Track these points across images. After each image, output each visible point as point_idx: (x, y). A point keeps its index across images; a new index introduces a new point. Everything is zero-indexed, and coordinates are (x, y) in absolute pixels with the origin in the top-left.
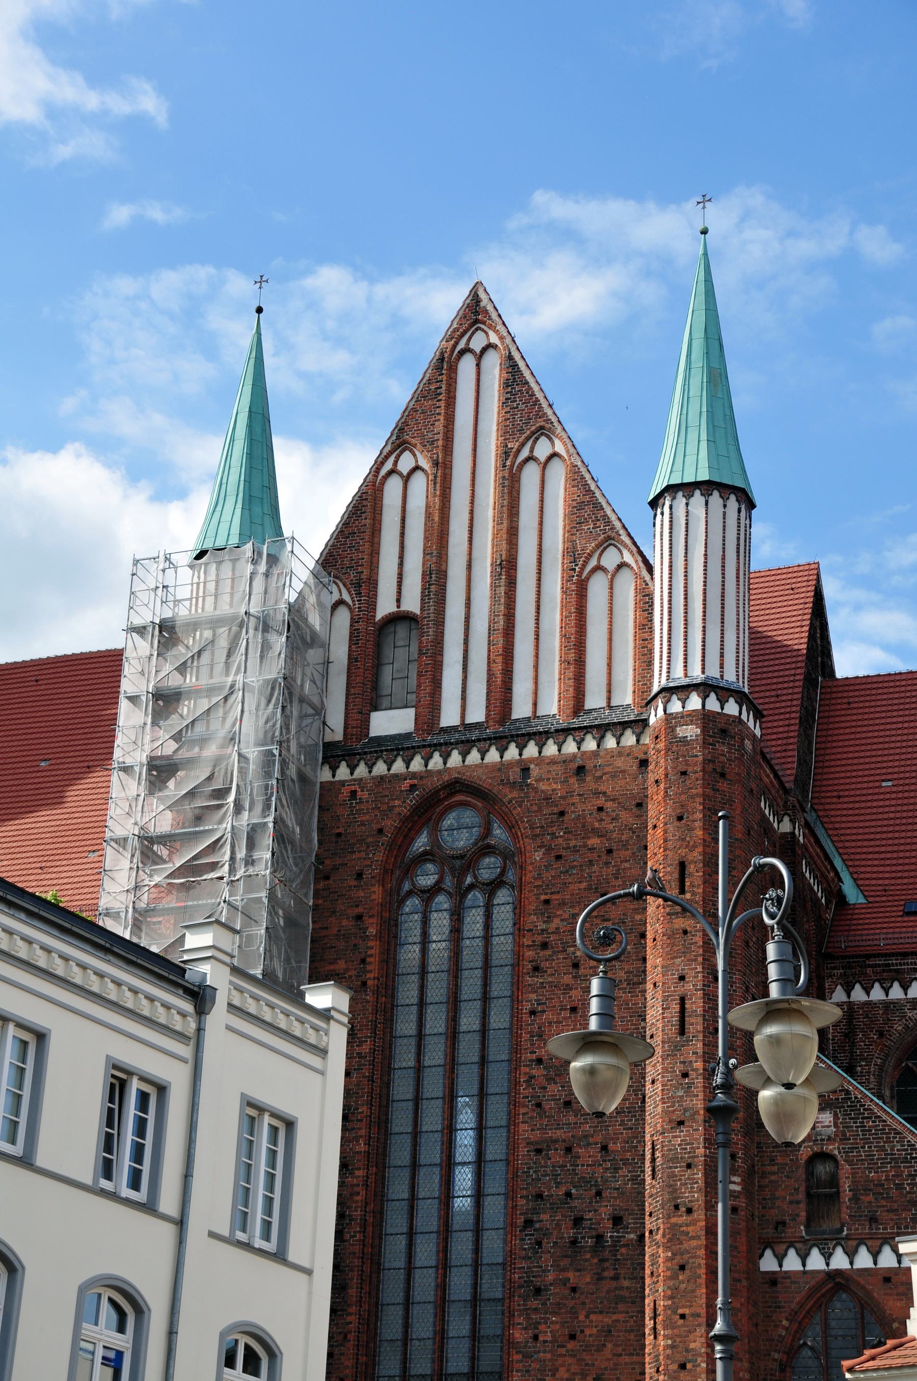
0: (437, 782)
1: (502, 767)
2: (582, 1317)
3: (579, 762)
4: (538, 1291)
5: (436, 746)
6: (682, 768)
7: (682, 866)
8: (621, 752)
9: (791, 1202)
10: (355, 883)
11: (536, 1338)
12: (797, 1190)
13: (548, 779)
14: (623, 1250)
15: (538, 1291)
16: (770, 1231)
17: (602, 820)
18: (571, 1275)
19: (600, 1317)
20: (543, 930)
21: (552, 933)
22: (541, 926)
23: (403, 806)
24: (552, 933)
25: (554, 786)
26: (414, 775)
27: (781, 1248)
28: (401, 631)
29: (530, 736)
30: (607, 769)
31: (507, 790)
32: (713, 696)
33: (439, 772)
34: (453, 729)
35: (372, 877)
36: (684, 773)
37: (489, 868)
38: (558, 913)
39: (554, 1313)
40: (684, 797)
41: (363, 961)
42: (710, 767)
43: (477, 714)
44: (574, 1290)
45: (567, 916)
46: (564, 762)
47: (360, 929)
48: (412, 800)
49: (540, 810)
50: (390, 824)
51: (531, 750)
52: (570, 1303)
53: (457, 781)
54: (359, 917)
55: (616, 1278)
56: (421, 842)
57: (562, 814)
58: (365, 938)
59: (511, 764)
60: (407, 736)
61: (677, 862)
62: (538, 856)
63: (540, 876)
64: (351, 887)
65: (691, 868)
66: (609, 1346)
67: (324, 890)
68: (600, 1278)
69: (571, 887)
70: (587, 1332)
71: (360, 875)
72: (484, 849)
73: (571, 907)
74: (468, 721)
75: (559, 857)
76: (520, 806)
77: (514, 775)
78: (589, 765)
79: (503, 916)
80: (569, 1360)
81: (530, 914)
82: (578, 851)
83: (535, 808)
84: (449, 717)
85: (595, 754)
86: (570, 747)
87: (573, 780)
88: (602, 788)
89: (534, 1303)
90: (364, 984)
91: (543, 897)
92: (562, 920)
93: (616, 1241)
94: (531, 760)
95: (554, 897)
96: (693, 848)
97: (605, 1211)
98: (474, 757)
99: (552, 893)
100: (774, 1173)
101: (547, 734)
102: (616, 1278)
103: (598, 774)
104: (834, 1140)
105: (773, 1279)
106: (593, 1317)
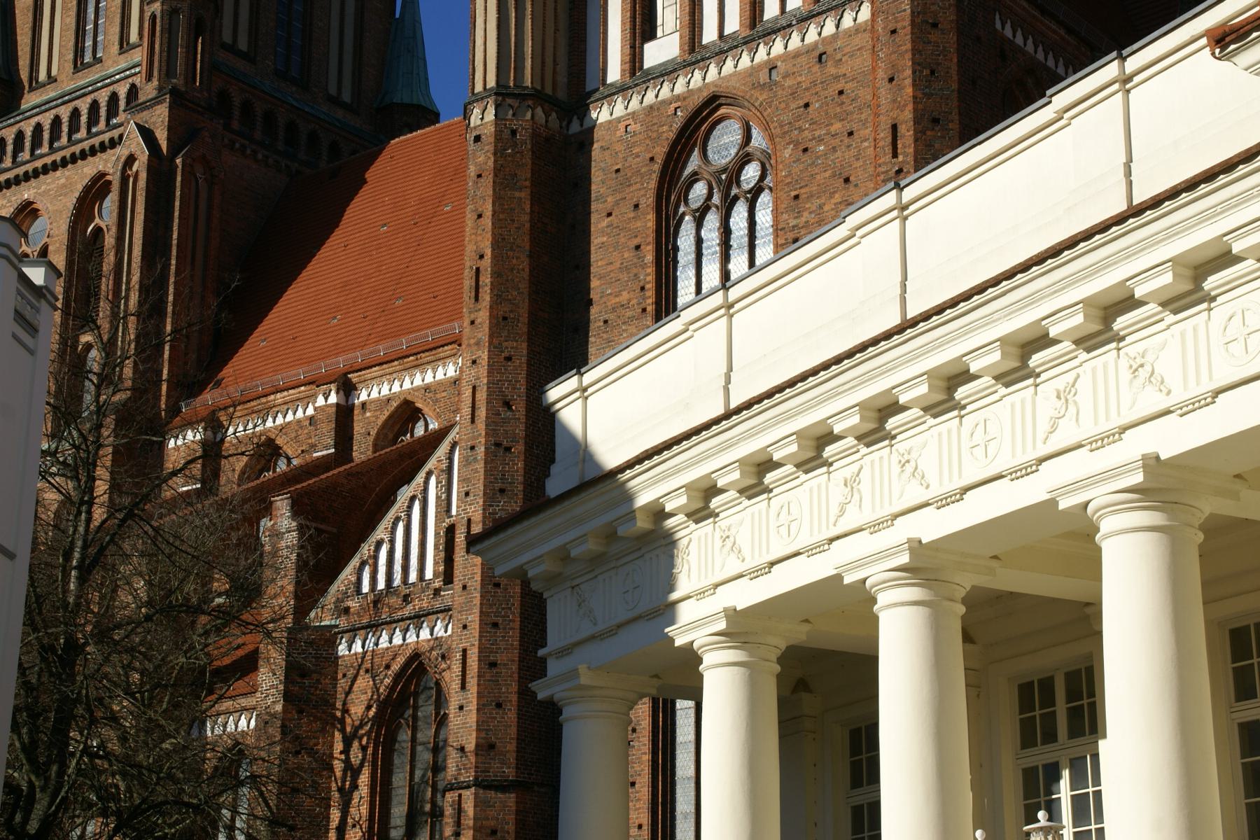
0: (697, 100)
1: (753, 71)
3: (821, 49)
6: (891, 27)
7: (894, 128)
8: (857, 30)
10: (632, 215)
13: (794, 73)
17: (843, 103)
20: (793, 227)
21: (802, 227)
22: (793, 222)
23: (669, 132)
24: (802, 227)
25: (799, 79)
30: (847, 50)
31: (756, 94)
33: (700, 89)
35: (647, 206)
36: (894, 32)
37: (751, 173)
38: (807, 206)
40: (894, 56)
41: (643, 288)
42: (919, 20)
45: (814, 208)
46: (807, 52)
47: (639, 258)
48: (677, 124)
49: (787, 105)
50: (661, 151)
54: (638, 247)
56: (694, 163)
57: (807, 105)
58: (644, 267)
61: (889, 126)
62: (787, 153)
63: (790, 174)
64: (629, 219)
65: (902, 129)
67: (607, 227)
69: (818, 177)
71: (636, 206)
72: (744, 159)
73: (818, 198)
75: (805, 150)
76: (770, 107)
77: (763, 77)
78: (830, 50)
79: (764, 217)
81: (782, 213)
82: (823, 139)
83: (783, 105)
85: (834, 37)
86: (812, 36)
87: (816, 68)
88: (842, 70)
90: (644, 310)
91: (793, 194)
92: (810, 213)
94: (779, 57)
95: (803, 191)
96: (902, 108)
99: (801, 188)
103: (838, 56)
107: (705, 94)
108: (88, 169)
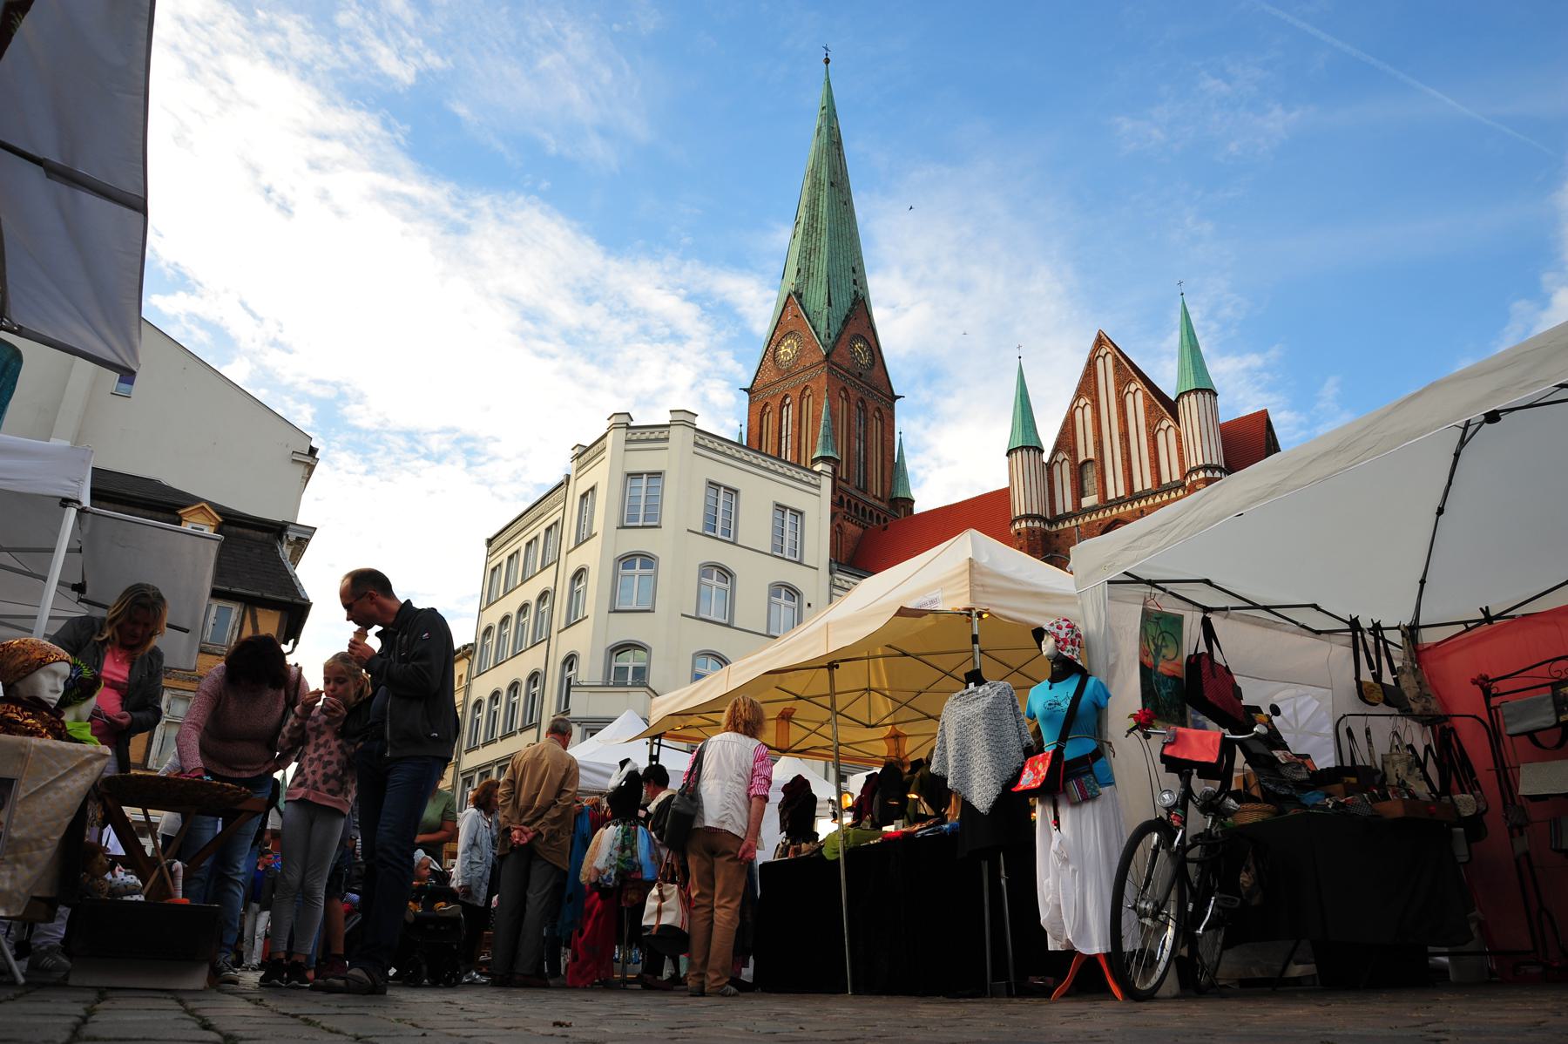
5: (1106, 507)
26: (1100, 520)
28: (1089, 465)
29: (1142, 498)
32: (1209, 471)
34: (1113, 500)
43: (1121, 493)
51: (1143, 503)
53: (1116, 520)
59: (1136, 510)
60: (1096, 506)
74: (1118, 496)
84: (1111, 496)
94: (1143, 507)
98: (1122, 509)
101: (1148, 496)
107: (1112, 519)
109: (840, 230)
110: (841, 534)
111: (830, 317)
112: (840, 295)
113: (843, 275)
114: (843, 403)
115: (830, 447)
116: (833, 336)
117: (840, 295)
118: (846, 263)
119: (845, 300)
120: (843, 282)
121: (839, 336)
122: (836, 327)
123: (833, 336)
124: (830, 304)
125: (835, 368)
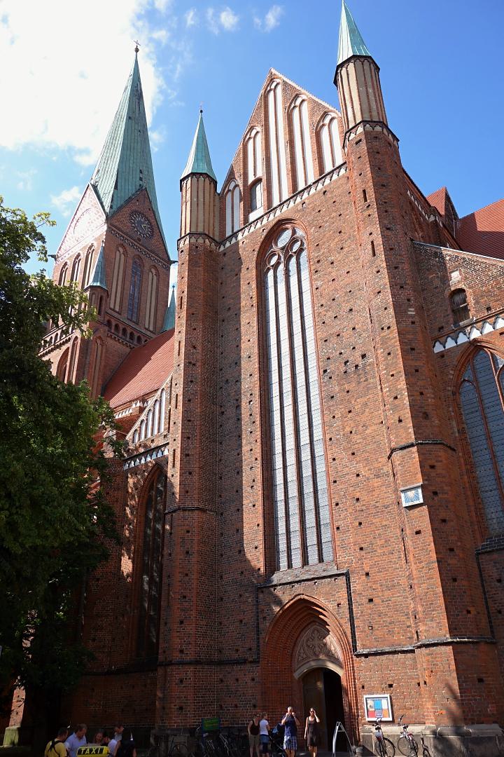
2: (353, 402)
4: (332, 397)
9: (444, 317)
11: (334, 417)
12: (447, 310)
14: (368, 368)
15: (332, 397)
16: (436, 333)
18: (347, 387)
19: (361, 399)
27: (442, 340)
39: (341, 404)
44: (348, 392)
52: (347, 398)
55: (366, 380)
66: (367, 410)
68: (359, 383)
70: (356, 408)
80: (350, 422)
89: (331, 403)
93: (364, 366)
97: (358, 354)
100: (433, 307)
102: (366, 380)
104: (461, 281)
105: (442, 355)
106: (358, 400)
108: (64, 348)
109: (132, 144)
110: (102, 346)
111: (115, 196)
112: (127, 184)
113: (131, 173)
114: (120, 256)
115: (99, 279)
116: (114, 207)
117: (127, 184)
118: (135, 165)
119: (130, 188)
120: (131, 177)
121: (120, 209)
122: (118, 203)
123: (114, 207)
124: (116, 187)
125: (114, 229)
